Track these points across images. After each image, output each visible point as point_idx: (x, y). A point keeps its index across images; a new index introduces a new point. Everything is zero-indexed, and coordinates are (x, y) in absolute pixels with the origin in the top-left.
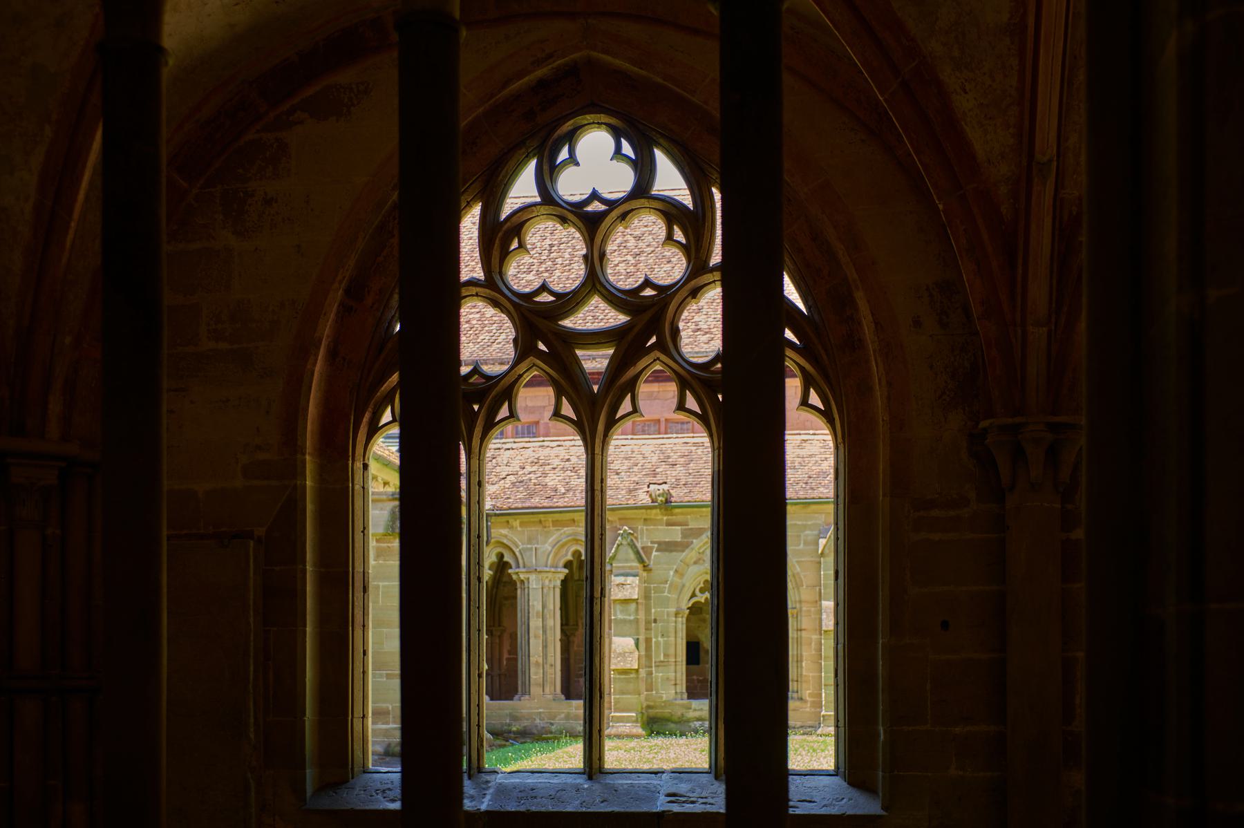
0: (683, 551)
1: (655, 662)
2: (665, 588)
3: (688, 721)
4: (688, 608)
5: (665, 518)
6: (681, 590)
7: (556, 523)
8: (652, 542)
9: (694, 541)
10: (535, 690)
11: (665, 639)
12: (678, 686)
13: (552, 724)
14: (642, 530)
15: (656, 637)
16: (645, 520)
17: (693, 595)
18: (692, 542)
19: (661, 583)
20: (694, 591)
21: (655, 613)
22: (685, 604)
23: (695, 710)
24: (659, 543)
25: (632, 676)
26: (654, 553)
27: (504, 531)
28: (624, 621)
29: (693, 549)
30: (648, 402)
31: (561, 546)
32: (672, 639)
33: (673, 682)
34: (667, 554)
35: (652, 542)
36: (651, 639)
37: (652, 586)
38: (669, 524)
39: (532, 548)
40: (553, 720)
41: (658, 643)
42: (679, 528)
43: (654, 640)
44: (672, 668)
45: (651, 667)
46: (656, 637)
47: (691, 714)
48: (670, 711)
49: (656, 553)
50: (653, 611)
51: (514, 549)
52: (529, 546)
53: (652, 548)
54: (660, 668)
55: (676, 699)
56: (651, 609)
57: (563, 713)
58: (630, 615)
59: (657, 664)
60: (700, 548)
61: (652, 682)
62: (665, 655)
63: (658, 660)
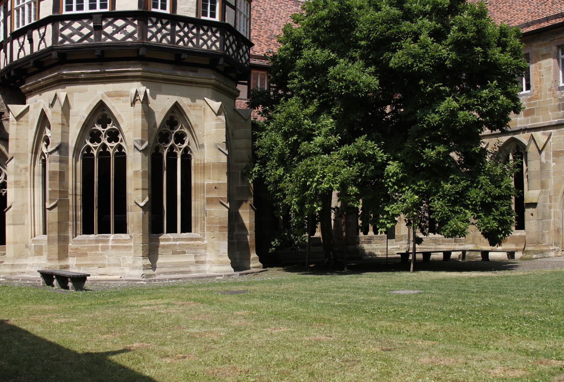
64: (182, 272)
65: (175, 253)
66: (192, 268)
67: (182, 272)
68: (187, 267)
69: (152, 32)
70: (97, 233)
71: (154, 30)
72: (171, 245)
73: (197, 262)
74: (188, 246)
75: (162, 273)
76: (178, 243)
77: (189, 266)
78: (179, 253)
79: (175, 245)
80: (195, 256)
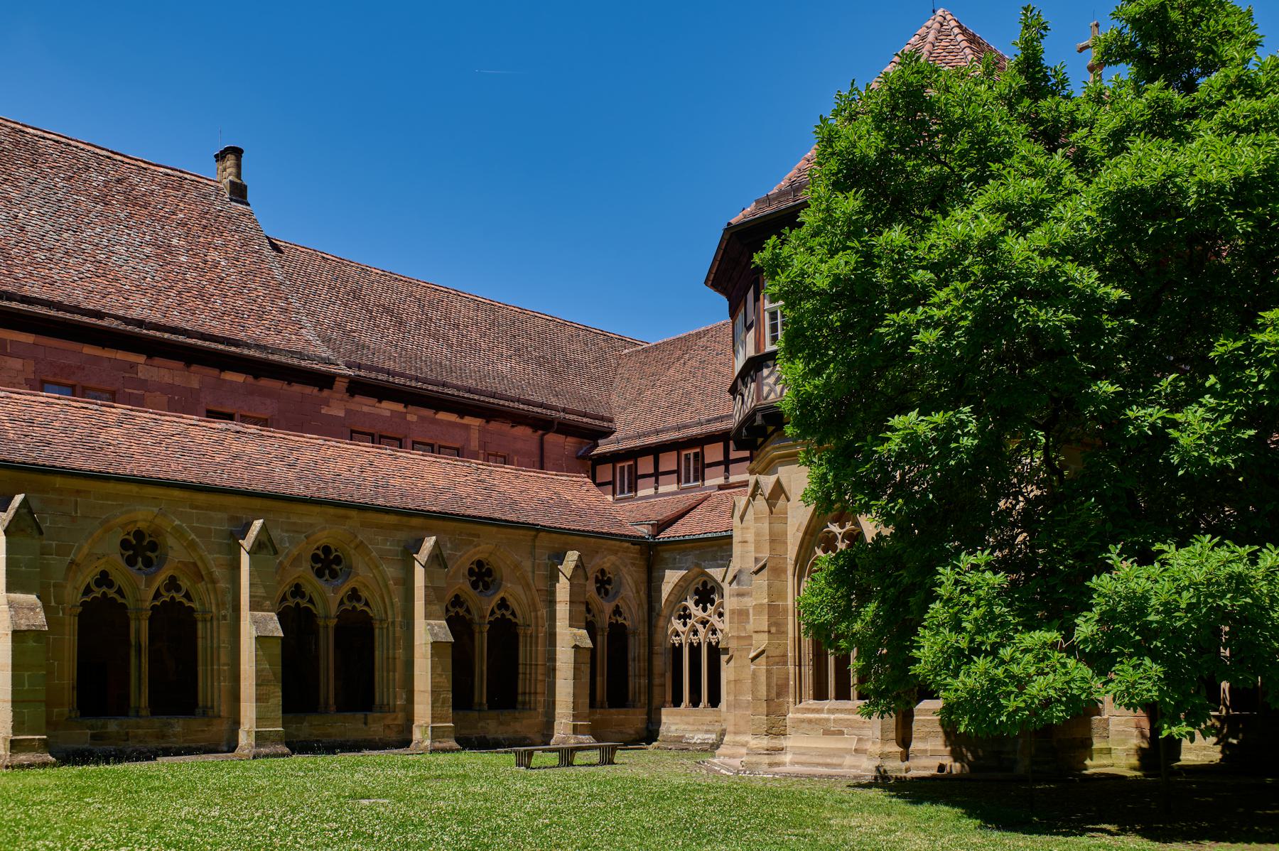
64: (827, 765)
65: (827, 732)
66: (849, 760)
67: (827, 765)
68: (841, 757)
69: (769, 385)
70: (855, 697)
71: (771, 380)
72: (821, 719)
73: (856, 750)
74: (848, 722)
75: (797, 763)
76: (832, 717)
77: (844, 757)
78: (833, 733)
79: (828, 720)
80: (860, 740)
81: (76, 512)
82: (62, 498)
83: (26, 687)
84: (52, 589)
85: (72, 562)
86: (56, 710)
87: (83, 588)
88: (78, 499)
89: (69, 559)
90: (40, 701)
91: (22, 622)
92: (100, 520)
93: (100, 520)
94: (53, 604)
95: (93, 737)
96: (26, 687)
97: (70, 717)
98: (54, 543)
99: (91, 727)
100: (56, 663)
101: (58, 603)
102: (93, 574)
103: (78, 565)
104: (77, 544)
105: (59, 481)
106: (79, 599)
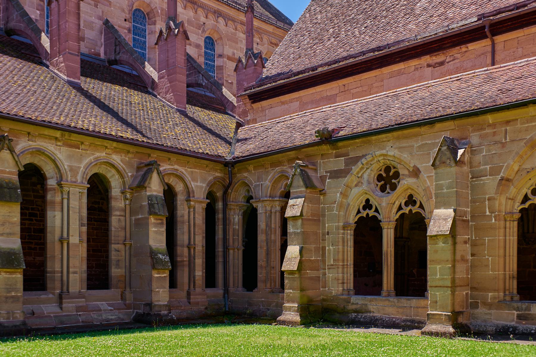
0: (346, 177)
1: (328, 266)
2: (334, 207)
3: (348, 312)
4: (355, 223)
5: (334, 152)
6: (347, 208)
7: (274, 165)
8: (326, 172)
9: (353, 167)
10: (260, 285)
11: (334, 247)
12: (345, 285)
13: (268, 310)
14: (320, 162)
15: (329, 246)
16: (322, 155)
17: (359, 212)
18: (352, 169)
19: (331, 204)
20: (359, 210)
21: (328, 227)
22: (352, 219)
23: (353, 304)
24: (330, 172)
25: (296, 276)
26: (328, 180)
27: (245, 175)
28: (295, 233)
29: (352, 174)
30: (398, 77)
31: (276, 182)
32: (341, 247)
33: (340, 281)
34: (335, 180)
35: (326, 172)
36: (325, 247)
37: (326, 206)
38: (337, 156)
39: (259, 184)
40: (270, 306)
41: (329, 250)
42: (343, 158)
43: (327, 248)
44: (340, 270)
45: (326, 269)
46: (329, 246)
47: (350, 307)
48: (336, 303)
49: (329, 180)
50: (327, 225)
51: (251, 186)
52: (258, 183)
53: (326, 176)
54: (331, 270)
55: (342, 295)
56: (325, 224)
57: (275, 301)
58: (298, 229)
59: (329, 267)
60: (358, 173)
61: (326, 281)
62: (333, 260)
63: (329, 264)
81: (506, 139)
82: (495, 130)
83: (438, 277)
84: (487, 203)
85: (502, 179)
86: (490, 294)
87: (520, 198)
88: (508, 128)
89: (499, 177)
90: (447, 287)
91: (435, 229)
92: (525, 141)
93: (525, 141)
94: (488, 213)
95: (519, 317)
96: (438, 277)
97: (505, 300)
98: (488, 167)
99: (518, 309)
100: (490, 258)
101: (491, 212)
102: (529, 185)
103: (508, 180)
104: (505, 164)
105: (490, 118)
106: (518, 207)
